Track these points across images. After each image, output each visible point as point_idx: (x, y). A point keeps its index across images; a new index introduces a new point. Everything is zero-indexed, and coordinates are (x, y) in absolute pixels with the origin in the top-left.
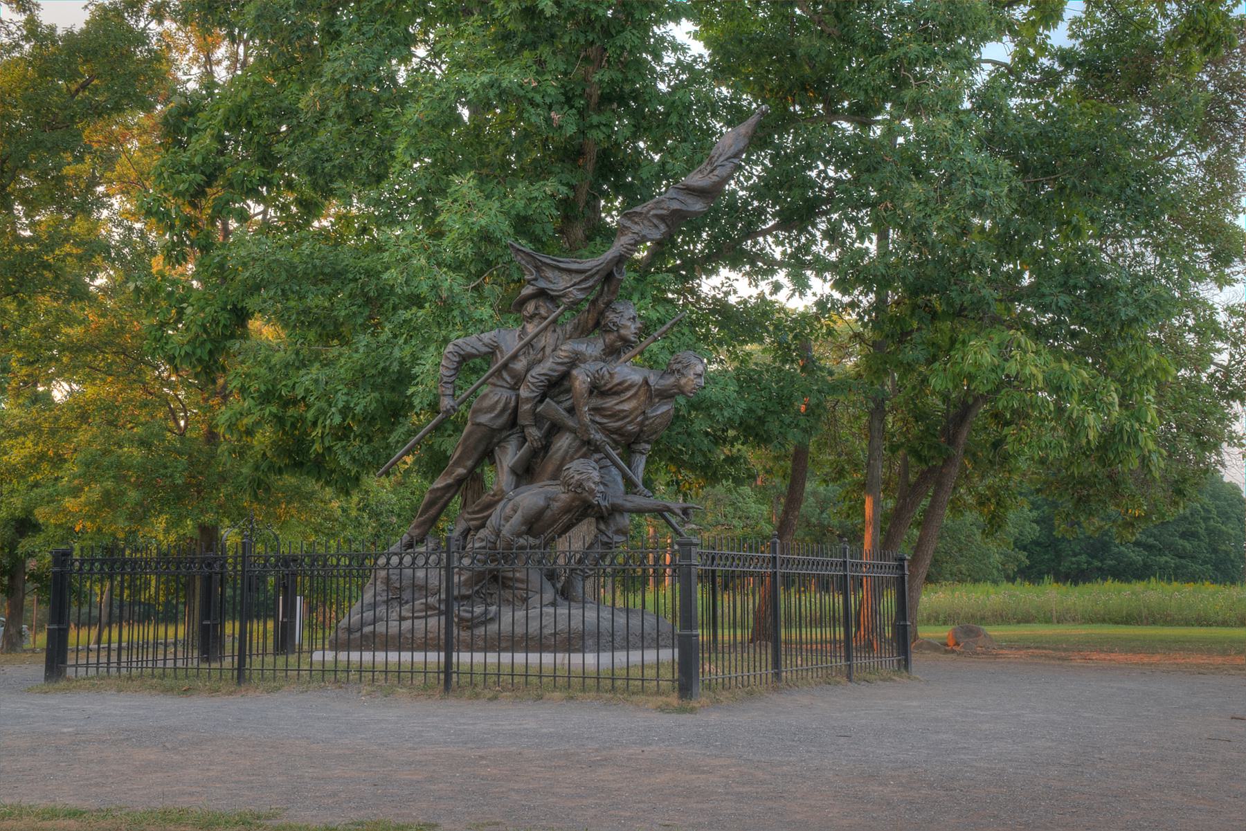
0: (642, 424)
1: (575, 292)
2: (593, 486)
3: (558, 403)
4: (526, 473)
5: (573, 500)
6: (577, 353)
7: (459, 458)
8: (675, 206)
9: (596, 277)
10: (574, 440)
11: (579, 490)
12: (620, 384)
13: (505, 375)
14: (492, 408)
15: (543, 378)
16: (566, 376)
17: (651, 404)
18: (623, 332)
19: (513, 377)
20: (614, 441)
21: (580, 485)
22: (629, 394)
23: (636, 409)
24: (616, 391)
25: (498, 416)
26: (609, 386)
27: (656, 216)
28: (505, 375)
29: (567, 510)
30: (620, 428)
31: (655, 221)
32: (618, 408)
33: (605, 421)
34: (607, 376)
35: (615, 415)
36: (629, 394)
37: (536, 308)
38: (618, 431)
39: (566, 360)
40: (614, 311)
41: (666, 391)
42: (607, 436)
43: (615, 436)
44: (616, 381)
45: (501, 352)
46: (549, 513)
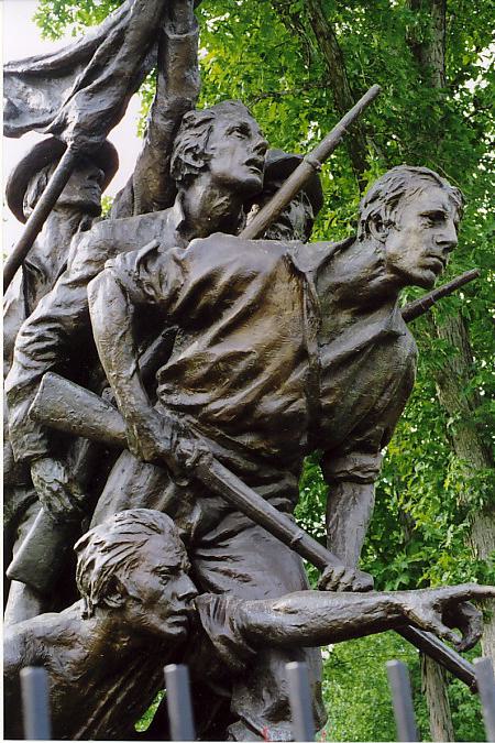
0: (310, 388)
2: (153, 582)
5: (111, 633)
9: (123, 51)
10: (138, 472)
12: (207, 282)
17: (329, 335)
18: (217, 166)
23: (274, 346)
24: (201, 308)
30: (247, 409)
33: (200, 398)
38: (244, 418)
41: (361, 283)
42: (222, 441)
43: (247, 440)
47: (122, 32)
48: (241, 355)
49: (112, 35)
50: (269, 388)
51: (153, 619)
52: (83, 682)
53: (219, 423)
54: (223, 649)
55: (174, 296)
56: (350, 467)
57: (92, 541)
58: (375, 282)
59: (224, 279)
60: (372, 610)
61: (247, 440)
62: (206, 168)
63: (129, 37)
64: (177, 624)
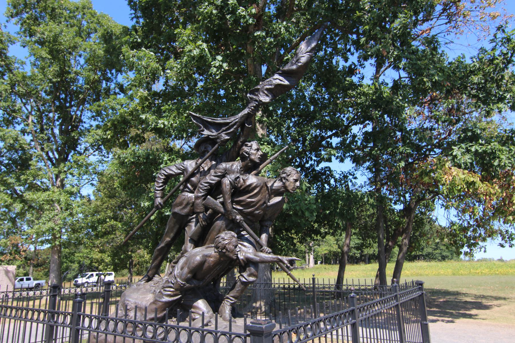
1: (223, 135)
3: (216, 199)
4: (199, 241)
6: (226, 170)
7: (167, 232)
8: (278, 82)
11: (224, 251)
12: (250, 185)
13: (189, 185)
14: (181, 204)
15: (206, 184)
16: (219, 184)
18: (253, 157)
19: (192, 186)
20: (249, 219)
21: (224, 248)
22: (256, 191)
23: (259, 201)
26: (243, 187)
27: (267, 89)
28: (189, 185)
29: (217, 263)
31: (266, 92)
32: (249, 200)
34: (242, 181)
35: (248, 205)
36: (256, 191)
37: (205, 148)
39: (220, 174)
40: (246, 145)
43: (249, 217)
44: (248, 183)
45: (187, 172)
46: (206, 265)
47: (236, 122)
48: (252, 202)
50: (257, 209)
51: (231, 255)
52: (213, 265)
53: (245, 213)
54: (242, 261)
55: (241, 186)
59: (253, 186)
60: (274, 259)
61: (249, 217)
62: (249, 157)
63: (238, 124)
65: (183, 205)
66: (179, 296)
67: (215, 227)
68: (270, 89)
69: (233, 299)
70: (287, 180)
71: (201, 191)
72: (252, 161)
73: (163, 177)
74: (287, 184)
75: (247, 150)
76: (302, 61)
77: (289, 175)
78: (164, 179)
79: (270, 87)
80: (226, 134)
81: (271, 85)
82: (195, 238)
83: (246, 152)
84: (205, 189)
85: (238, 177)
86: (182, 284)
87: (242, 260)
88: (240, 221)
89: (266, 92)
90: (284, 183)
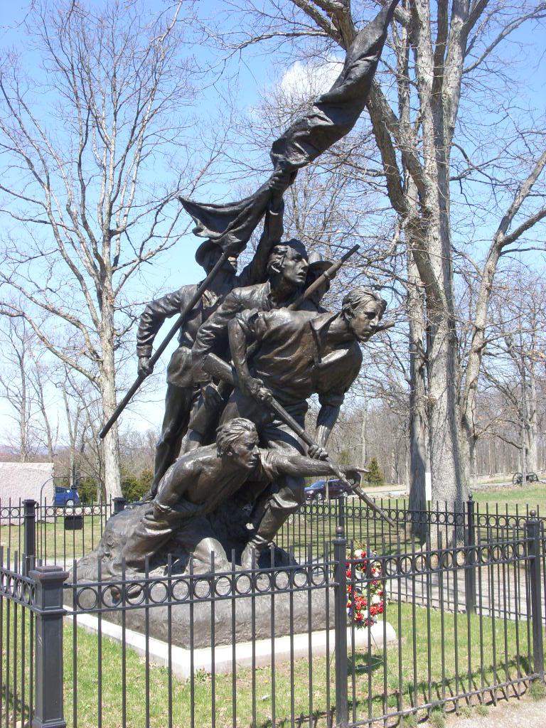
15: (208, 332)
18: (289, 274)
23: (300, 358)
25: (181, 375)
49: (245, 209)
50: (298, 374)
51: (243, 462)
54: (269, 473)
55: (262, 333)
56: (329, 401)
57: (223, 430)
58: (345, 335)
62: (282, 273)
64: (252, 464)
65: (181, 370)
66: (169, 530)
67: (228, 410)
68: (303, 136)
69: (261, 538)
70: (353, 315)
71: (202, 344)
72: (288, 281)
73: (150, 320)
74: (354, 322)
75: (278, 261)
76: (353, 76)
77: (356, 305)
78: (150, 323)
79: (303, 133)
80: (235, 234)
81: (305, 130)
82: (202, 430)
83: (277, 266)
84: (207, 341)
85: (256, 316)
86: (163, 509)
87: (269, 469)
88: (266, 399)
89: (297, 145)
90: (347, 322)
